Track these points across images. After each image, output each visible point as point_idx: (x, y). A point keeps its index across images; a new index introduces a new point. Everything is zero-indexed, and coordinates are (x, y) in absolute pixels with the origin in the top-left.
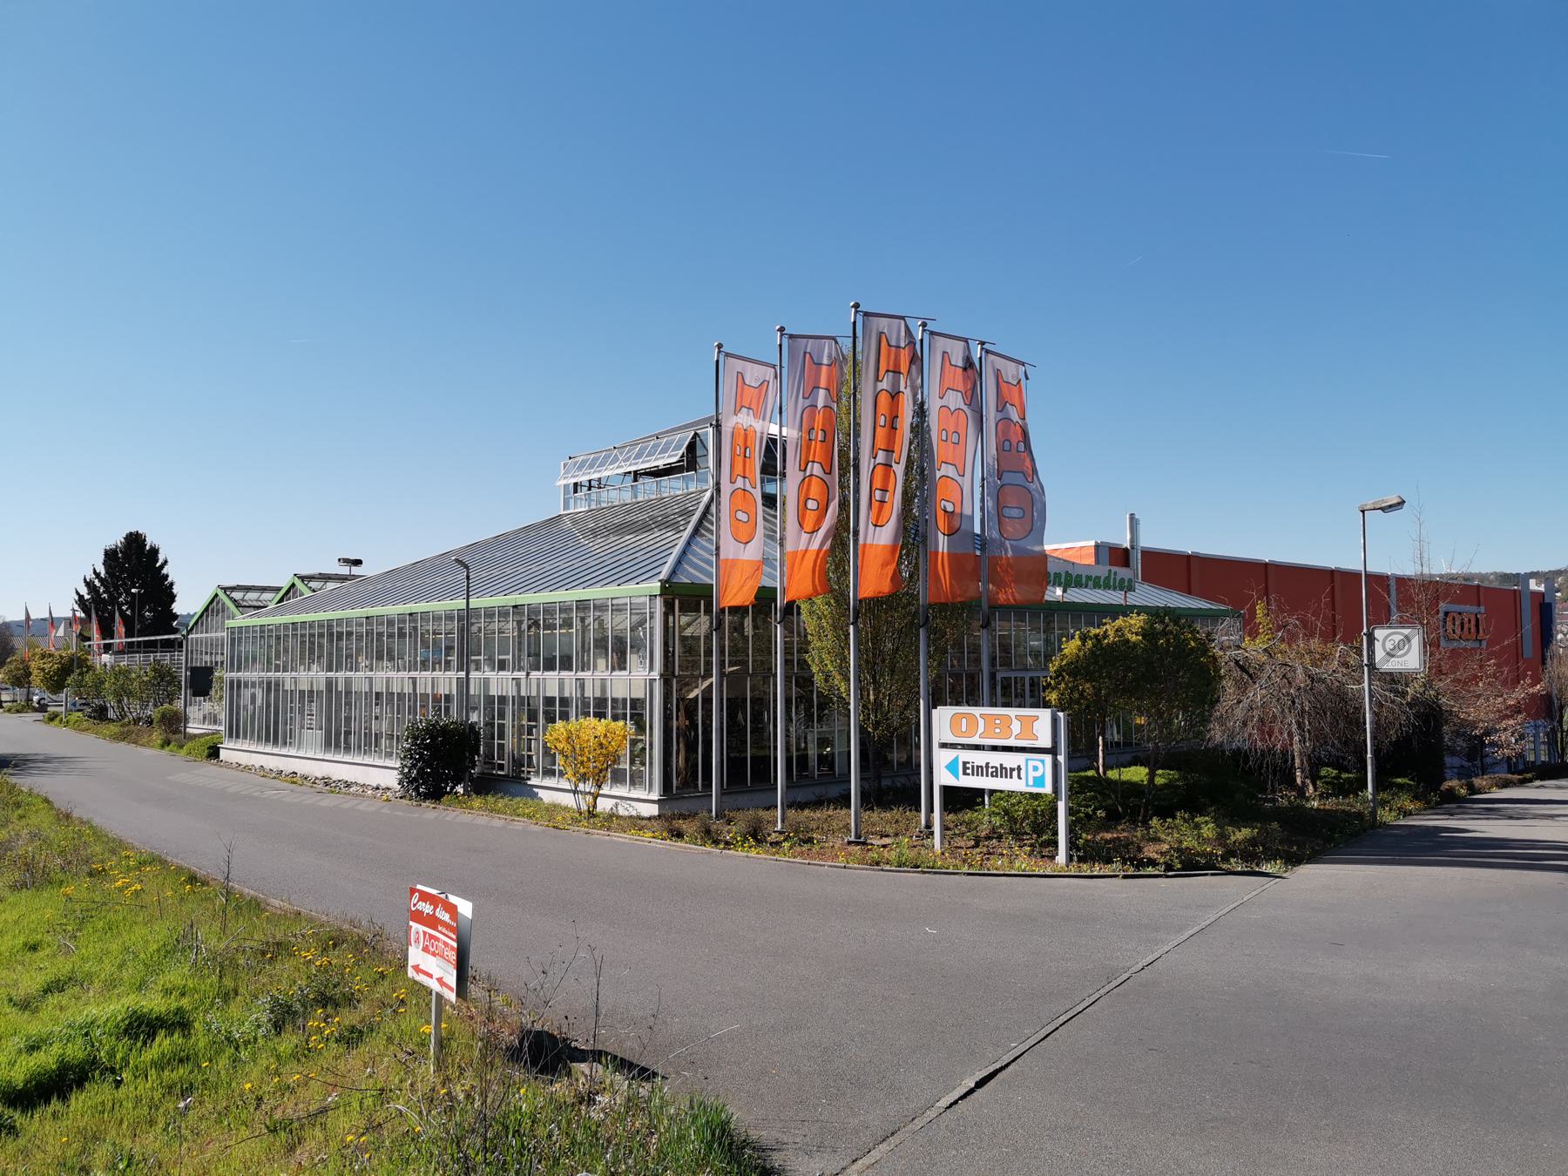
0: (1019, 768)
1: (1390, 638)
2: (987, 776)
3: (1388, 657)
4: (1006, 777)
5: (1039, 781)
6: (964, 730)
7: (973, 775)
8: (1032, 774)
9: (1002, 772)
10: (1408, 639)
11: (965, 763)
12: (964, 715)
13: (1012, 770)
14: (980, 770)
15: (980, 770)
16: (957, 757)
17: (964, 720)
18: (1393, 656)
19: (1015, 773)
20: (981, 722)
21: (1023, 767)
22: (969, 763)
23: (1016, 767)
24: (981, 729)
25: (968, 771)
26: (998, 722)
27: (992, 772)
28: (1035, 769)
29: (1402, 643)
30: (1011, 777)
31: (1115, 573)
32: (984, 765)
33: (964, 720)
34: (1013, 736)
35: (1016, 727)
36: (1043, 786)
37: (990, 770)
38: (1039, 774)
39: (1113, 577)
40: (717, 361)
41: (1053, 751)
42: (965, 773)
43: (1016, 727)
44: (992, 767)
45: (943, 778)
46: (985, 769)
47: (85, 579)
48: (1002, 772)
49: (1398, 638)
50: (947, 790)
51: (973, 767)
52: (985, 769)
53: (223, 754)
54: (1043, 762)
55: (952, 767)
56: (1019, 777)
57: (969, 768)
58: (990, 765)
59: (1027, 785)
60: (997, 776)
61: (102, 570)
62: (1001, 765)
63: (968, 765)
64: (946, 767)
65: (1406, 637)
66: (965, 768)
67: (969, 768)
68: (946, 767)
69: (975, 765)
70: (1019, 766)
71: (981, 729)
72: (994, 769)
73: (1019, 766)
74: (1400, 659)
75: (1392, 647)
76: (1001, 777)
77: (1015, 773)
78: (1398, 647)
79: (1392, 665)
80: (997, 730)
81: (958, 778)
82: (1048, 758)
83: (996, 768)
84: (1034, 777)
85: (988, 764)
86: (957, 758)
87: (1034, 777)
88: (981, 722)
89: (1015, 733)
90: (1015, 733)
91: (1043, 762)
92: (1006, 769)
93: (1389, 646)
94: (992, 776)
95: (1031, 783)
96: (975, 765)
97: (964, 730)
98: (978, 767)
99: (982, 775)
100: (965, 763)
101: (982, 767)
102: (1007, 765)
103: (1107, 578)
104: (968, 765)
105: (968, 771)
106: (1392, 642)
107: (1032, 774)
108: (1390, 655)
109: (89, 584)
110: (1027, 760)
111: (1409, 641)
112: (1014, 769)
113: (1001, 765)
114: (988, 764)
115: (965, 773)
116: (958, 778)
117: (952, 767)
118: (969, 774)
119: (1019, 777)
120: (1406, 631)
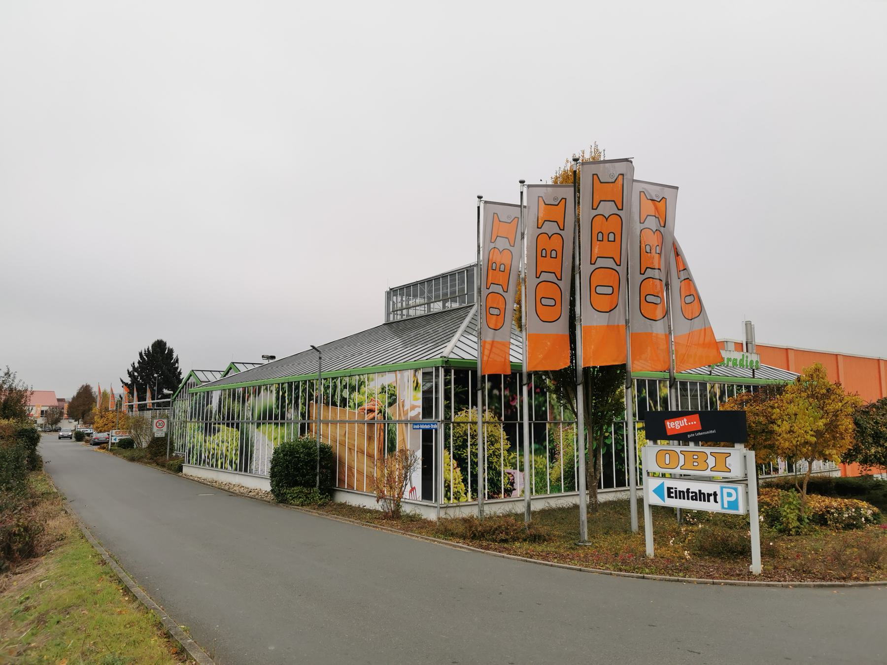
0: (715, 494)
2: (688, 499)
5: (734, 505)
6: (667, 463)
7: (676, 498)
11: (669, 489)
12: (667, 452)
13: (709, 495)
14: (681, 495)
15: (681, 495)
16: (664, 482)
17: (667, 456)
19: (712, 498)
20: (682, 457)
21: (718, 493)
22: (672, 488)
23: (713, 493)
24: (682, 463)
25: (672, 495)
27: (692, 496)
28: (729, 495)
30: (709, 501)
32: (685, 491)
33: (667, 456)
34: (709, 469)
35: (711, 461)
36: (737, 508)
37: (691, 495)
38: (733, 499)
39: (745, 359)
40: (479, 208)
41: (744, 481)
42: (669, 496)
43: (711, 461)
44: (692, 493)
45: (655, 500)
46: (686, 494)
47: (128, 371)
50: (654, 508)
51: (676, 491)
52: (686, 494)
53: (186, 470)
54: (736, 490)
55: (658, 491)
56: (716, 501)
57: (672, 493)
58: (690, 491)
59: (723, 507)
60: (696, 500)
61: (137, 365)
62: (700, 491)
63: (671, 490)
64: (653, 491)
66: (669, 493)
67: (672, 493)
68: (653, 491)
71: (682, 463)
72: (694, 494)
77: (712, 498)
80: (696, 464)
82: (740, 488)
83: (696, 493)
85: (688, 490)
86: (664, 482)
88: (682, 457)
91: (736, 490)
92: (704, 494)
94: (692, 499)
95: (726, 506)
96: (678, 490)
97: (667, 463)
98: (680, 492)
99: (684, 498)
100: (669, 489)
101: (683, 492)
103: (742, 360)
104: (671, 490)
105: (672, 495)
109: (130, 374)
110: (722, 488)
112: (711, 495)
113: (700, 491)
114: (688, 490)
115: (669, 496)
117: (658, 491)
118: (673, 497)
119: (716, 501)
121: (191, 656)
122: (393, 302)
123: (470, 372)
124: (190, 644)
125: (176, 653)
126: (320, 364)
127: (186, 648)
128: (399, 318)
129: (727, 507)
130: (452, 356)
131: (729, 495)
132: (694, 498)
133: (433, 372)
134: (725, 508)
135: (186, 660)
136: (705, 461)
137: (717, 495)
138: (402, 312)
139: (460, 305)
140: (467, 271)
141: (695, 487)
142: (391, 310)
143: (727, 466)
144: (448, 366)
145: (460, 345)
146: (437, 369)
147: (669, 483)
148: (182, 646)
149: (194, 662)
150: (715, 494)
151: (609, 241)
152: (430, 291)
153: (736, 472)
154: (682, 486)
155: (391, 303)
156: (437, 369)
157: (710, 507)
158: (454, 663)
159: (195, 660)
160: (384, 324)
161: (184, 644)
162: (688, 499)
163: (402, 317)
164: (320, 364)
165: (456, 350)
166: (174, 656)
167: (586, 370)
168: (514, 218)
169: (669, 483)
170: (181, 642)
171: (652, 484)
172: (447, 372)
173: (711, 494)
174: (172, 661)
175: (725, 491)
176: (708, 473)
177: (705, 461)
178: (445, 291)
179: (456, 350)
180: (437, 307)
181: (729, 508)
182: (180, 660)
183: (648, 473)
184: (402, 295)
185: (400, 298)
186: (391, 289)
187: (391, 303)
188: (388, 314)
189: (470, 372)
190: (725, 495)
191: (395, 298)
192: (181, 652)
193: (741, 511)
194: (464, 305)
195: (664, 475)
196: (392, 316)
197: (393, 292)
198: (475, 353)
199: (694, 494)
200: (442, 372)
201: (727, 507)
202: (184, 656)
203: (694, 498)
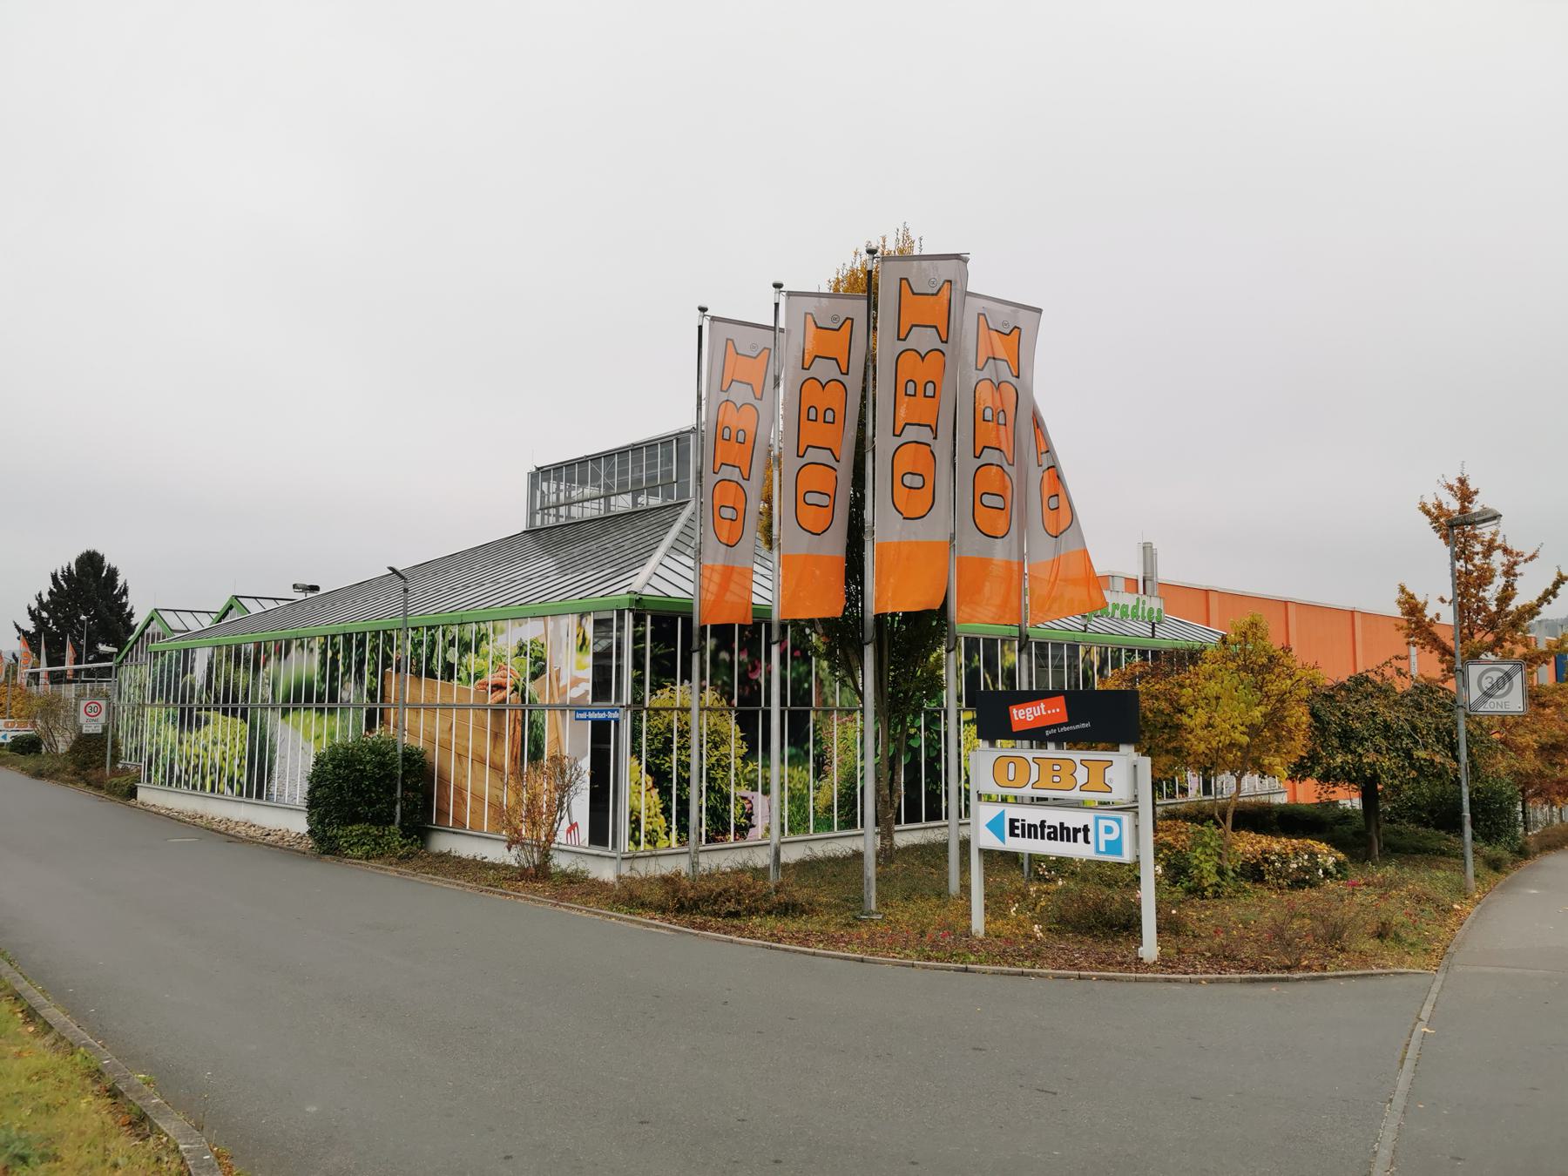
0: (1086, 829)
1: (1487, 675)
2: (1043, 838)
3: (1486, 698)
4: (1068, 840)
5: (1114, 846)
6: (1011, 778)
7: (1023, 836)
8: (1103, 837)
9: (1063, 833)
10: (1508, 676)
11: (1012, 821)
13: (1076, 831)
14: (1032, 831)
15: (1032, 831)
16: (1003, 812)
17: (1012, 766)
18: (1491, 696)
19: (1080, 836)
20: (1035, 768)
22: (1018, 820)
24: (1034, 778)
25: (1017, 831)
26: (1057, 768)
27: (1049, 834)
28: (1109, 830)
29: (1501, 682)
30: (1075, 840)
31: (1144, 602)
32: (1038, 824)
33: (1012, 766)
34: (1078, 787)
35: (1081, 775)
36: (1120, 854)
37: (1047, 831)
38: (1113, 837)
39: (1141, 606)
40: (700, 328)
41: (1133, 809)
42: (1012, 834)
43: (1081, 775)
44: (1049, 827)
45: (986, 839)
46: (1039, 829)
47: (29, 609)
49: (1496, 675)
50: (987, 854)
51: (1023, 825)
52: (1039, 829)
53: (144, 795)
54: (1119, 821)
55: (994, 825)
56: (1086, 841)
57: (1017, 828)
58: (1046, 824)
59: (1098, 851)
60: (1055, 839)
61: (46, 598)
62: (1062, 824)
63: (1016, 824)
64: (987, 825)
65: (1507, 674)
66: (1013, 828)
67: (1017, 828)
68: (987, 825)
69: (1026, 823)
70: (1086, 826)
71: (1034, 778)
72: (1052, 830)
73: (1086, 826)
74: (1499, 701)
75: (1489, 686)
76: (1062, 840)
77: (1080, 836)
78: (1497, 685)
79: (1491, 706)
81: (1003, 841)
82: (1126, 818)
83: (1055, 828)
84: (1107, 842)
85: (1043, 822)
86: (1004, 811)
87: (1107, 842)
88: (1035, 768)
91: (1119, 821)
92: (1068, 829)
93: (1486, 684)
94: (1050, 838)
95: (1102, 848)
96: (1026, 823)
97: (1011, 778)
98: (1030, 826)
99: (1036, 837)
100: (1012, 821)
101: (1035, 826)
102: (1070, 824)
103: (1135, 607)
104: (1016, 824)
105: (1017, 831)
106: (1490, 680)
108: (1487, 695)
110: (1097, 819)
111: (1510, 678)
112: (1079, 830)
113: (1062, 824)
114: (1043, 822)
115: (1012, 834)
116: (1003, 841)
117: (994, 825)
118: (1017, 835)
119: (1086, 841)
120: (1507, 668)
121: (159, 1128)
122: (543, 492)
123: (680, 619)
124: (157, 1106)
125: (130, 1124)
126: (406, 602)
127: (148, 1113)
128: (552, 521)
129: (1104, 850)
130: (648, 591)
131: (1109, 830)
132: (1052, 835)
133: (612, 620)
134: (1102, 853)
135: (149, 1136)
136: (1072, 775)
137: (1089, 830)
138: (558, 511)
139: (663, 501)
140: (677, 440)
141: (1054, 817)
142: (538, 507)
143: (1106, 782)
144: (639, 608)
145: (662, 571)
148: (141, 1110)
149: (165, 1139)
151: (925, 396)
152: (610, 475)
153: (1120, 791)
154: (1032, 816)
155: (539, 493)
157: (1077, 850)
158: (642, 1123)
159: (167, 1135)
160: (525, 532)
161: (145, 1106)
162: (1043, 838)
163: (557, 520)
164: (406, 602)
165: (655, 581)
166: (125, 1128)
167: (880, 619)
168: (762, 351)
170: (138, 1103)
171: (984, 813)
172: (639, 620)
173: (1080, 829)
174: (122, 1139)
175: (1102, 823)
176: (1075, 794)
177: (1072, 775)
178: (637, 475)
179: (655, 581)
180: (623, 503)
181: (1107, 852)
182: (138, 1135)
183: (980, 796)
184: (558, 480)
185: (555, 486)
186: (538, 469)
187: (539, 493)
188: (532, 514)
189: (680, 619)
191: (545, 484)
192: (140, 1124)
193: (1127, 857)
194: (670, 502)
195: (1004, 800)
196: (538, 517)
197: (541, 475)
198: (690, 588)
199: (1052, 830)
200: (629, 619)
201: (1104, 850)
202: (144, 1129)
203: (1052, 835)
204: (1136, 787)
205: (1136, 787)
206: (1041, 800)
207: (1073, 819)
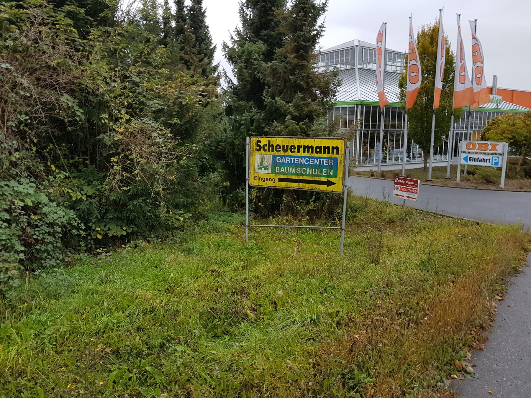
0: (490, 159)
6: (471, 147)
8: (494, 161)
9: (484, 160)
13: (487, 160)
14: (475, 160)
15: (475, 160)
16: (467, 156)
17: (471, 145)
19: (488, 161)
20: (478, 145)
24: (477, 147)
33: (471, 145)
35: (490, 147)
36: (498, 165)
42: (470, 161)
43: (490, 147)
48: (484, 160)
54: (498, 158)
55: (466, 159)
56: (489, 162)
59: (492, 164)
71: (477, 147)
82: (500, 157)
88: (478, 145)
89: (489, 149)
90: (489, 149)
91: (498, 158)
95: (493, 164)
97: (471, 147)
107: (494, 161)
110: (493, 157)
115: (470, 161)
117: (466, 159)
119: (489, 162)
130: (362, 99)
131: (495, 160)
133: (354, 107)
141: (481, 157)
146: (357, 106)
147: (470, 156)
150: (490, 159)
152: (328, 60)
153: (499, 151)
154: (475, 156)
156: (357, 106)
157: (487, 164)
169: (470, 156)
172: (362, 108)
175: (494, 158)
176: (488, 151)
178: (337, 60)
181: (495, 165)
190: (494, 160)
193: (499, 166)
195: (469, 153)
198: (378, 98)
200: (360, 107)
204: (504, 149)
205: (504, 149)
206: (477, 153)
207: (486, 157)
